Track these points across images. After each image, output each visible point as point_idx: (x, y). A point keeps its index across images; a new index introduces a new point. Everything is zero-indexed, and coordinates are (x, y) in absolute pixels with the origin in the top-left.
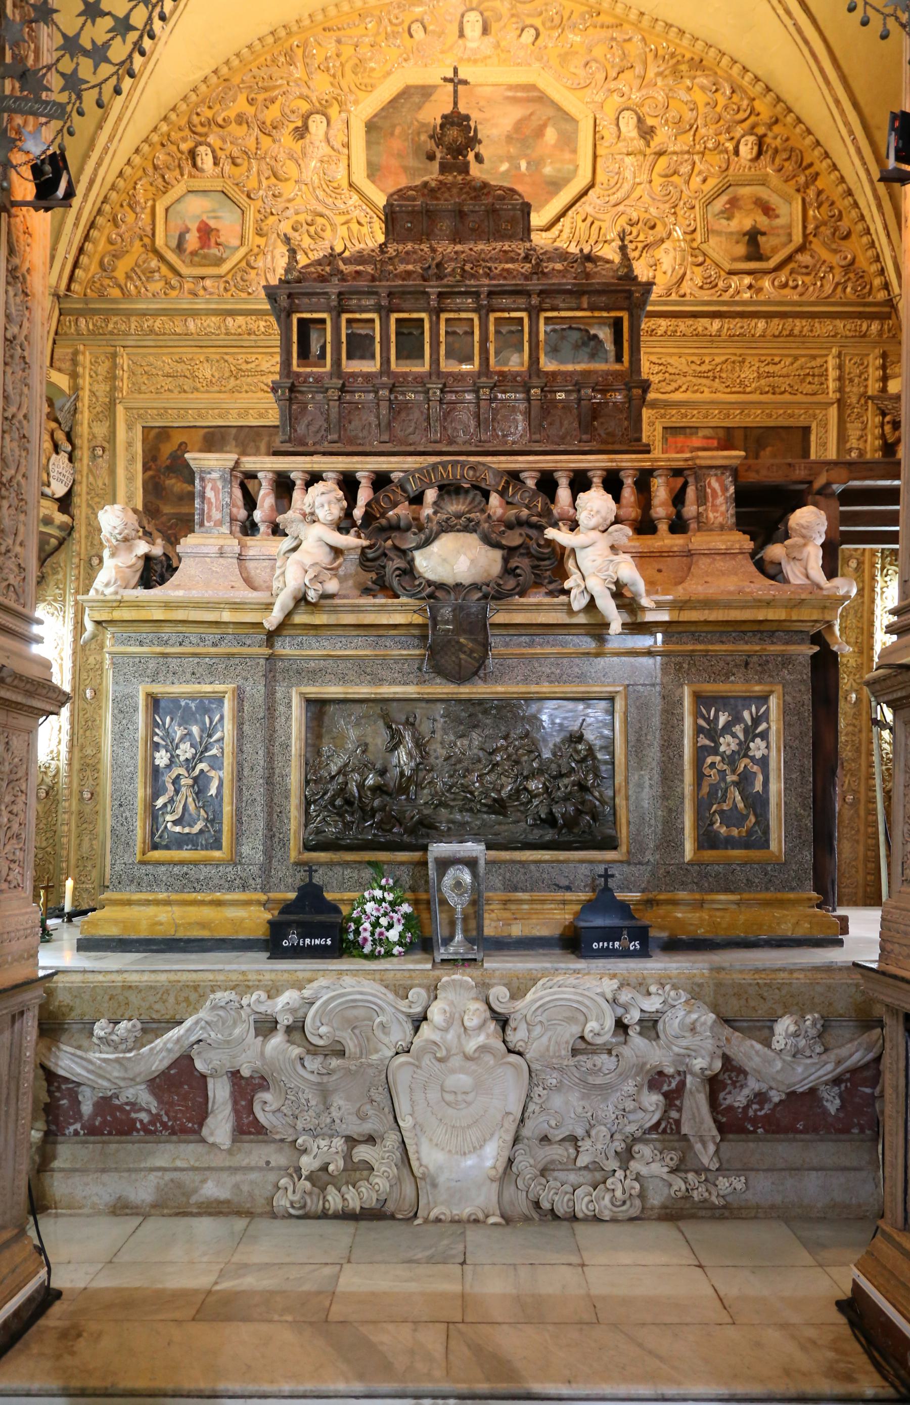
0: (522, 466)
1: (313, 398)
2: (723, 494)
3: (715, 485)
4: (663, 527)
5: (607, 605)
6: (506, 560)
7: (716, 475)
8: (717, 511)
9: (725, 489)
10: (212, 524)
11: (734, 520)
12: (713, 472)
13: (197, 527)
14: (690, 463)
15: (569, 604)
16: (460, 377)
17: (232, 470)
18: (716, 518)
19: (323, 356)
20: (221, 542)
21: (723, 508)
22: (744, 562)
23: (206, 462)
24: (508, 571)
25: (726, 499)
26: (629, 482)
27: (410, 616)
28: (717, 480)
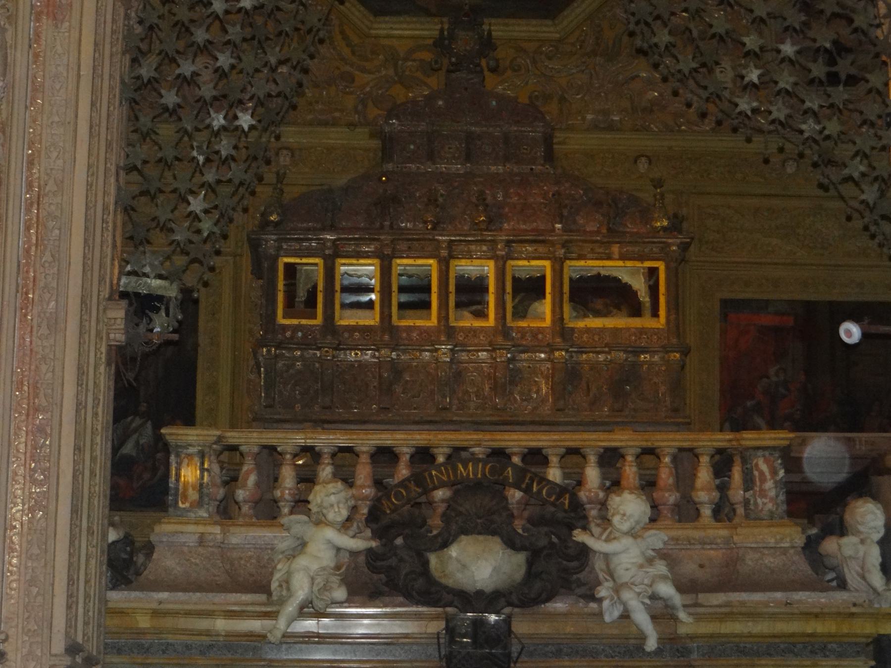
0: (544, 444)
1: (302, 356)
2: (773, 478)
3: (764, 467)
4: (707, 512)
5: (642, 618)
6: (530, 563)
7: (764, 456)
8: (765, 496)
9: (774, 472)
10: (187, 505)
11: (785, 507)
12: (760, 453)
13: (171, 510)
14: (734, 443)
15: (600, 614)
16: (473, 332)
17: (215, 443)
18: (764, 504)
19: (311, 302)
20: (201, 529)
21: (772, 493)
22: (796, 558)
23: (184, 438)
24: (531, 574)
25: (776, 482)
26: (667, 460)
27: (424, 623)
28: (766, 461)
